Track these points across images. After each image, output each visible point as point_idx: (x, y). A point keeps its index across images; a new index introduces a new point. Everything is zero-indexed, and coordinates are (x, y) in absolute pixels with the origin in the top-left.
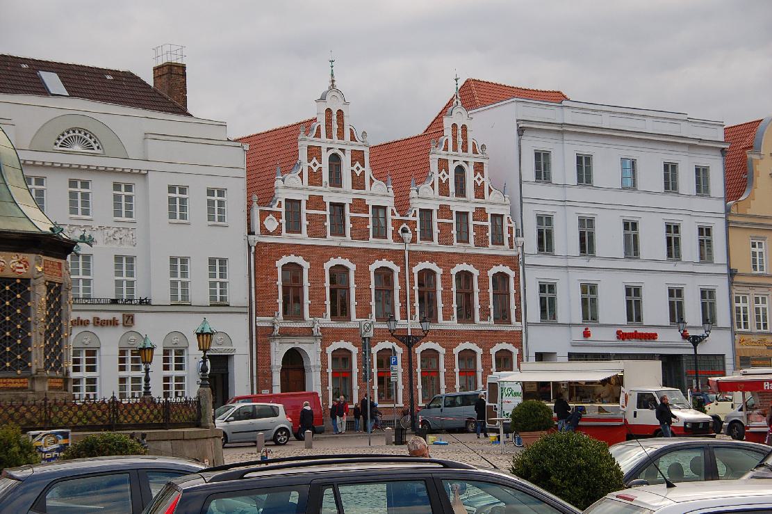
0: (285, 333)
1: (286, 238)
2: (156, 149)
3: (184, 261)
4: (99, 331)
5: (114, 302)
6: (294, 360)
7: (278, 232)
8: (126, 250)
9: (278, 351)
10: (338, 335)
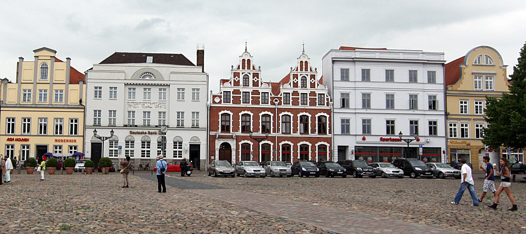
0: (221, 137)
1: (223, 105)
2: (173, 77)
3: (183, 113)
4: (150, 136)
5: (157, 126)
6: (226, 147)
7: (220, 102)
8: (162, 110)
9: (218, 144)
10: (244, 138)
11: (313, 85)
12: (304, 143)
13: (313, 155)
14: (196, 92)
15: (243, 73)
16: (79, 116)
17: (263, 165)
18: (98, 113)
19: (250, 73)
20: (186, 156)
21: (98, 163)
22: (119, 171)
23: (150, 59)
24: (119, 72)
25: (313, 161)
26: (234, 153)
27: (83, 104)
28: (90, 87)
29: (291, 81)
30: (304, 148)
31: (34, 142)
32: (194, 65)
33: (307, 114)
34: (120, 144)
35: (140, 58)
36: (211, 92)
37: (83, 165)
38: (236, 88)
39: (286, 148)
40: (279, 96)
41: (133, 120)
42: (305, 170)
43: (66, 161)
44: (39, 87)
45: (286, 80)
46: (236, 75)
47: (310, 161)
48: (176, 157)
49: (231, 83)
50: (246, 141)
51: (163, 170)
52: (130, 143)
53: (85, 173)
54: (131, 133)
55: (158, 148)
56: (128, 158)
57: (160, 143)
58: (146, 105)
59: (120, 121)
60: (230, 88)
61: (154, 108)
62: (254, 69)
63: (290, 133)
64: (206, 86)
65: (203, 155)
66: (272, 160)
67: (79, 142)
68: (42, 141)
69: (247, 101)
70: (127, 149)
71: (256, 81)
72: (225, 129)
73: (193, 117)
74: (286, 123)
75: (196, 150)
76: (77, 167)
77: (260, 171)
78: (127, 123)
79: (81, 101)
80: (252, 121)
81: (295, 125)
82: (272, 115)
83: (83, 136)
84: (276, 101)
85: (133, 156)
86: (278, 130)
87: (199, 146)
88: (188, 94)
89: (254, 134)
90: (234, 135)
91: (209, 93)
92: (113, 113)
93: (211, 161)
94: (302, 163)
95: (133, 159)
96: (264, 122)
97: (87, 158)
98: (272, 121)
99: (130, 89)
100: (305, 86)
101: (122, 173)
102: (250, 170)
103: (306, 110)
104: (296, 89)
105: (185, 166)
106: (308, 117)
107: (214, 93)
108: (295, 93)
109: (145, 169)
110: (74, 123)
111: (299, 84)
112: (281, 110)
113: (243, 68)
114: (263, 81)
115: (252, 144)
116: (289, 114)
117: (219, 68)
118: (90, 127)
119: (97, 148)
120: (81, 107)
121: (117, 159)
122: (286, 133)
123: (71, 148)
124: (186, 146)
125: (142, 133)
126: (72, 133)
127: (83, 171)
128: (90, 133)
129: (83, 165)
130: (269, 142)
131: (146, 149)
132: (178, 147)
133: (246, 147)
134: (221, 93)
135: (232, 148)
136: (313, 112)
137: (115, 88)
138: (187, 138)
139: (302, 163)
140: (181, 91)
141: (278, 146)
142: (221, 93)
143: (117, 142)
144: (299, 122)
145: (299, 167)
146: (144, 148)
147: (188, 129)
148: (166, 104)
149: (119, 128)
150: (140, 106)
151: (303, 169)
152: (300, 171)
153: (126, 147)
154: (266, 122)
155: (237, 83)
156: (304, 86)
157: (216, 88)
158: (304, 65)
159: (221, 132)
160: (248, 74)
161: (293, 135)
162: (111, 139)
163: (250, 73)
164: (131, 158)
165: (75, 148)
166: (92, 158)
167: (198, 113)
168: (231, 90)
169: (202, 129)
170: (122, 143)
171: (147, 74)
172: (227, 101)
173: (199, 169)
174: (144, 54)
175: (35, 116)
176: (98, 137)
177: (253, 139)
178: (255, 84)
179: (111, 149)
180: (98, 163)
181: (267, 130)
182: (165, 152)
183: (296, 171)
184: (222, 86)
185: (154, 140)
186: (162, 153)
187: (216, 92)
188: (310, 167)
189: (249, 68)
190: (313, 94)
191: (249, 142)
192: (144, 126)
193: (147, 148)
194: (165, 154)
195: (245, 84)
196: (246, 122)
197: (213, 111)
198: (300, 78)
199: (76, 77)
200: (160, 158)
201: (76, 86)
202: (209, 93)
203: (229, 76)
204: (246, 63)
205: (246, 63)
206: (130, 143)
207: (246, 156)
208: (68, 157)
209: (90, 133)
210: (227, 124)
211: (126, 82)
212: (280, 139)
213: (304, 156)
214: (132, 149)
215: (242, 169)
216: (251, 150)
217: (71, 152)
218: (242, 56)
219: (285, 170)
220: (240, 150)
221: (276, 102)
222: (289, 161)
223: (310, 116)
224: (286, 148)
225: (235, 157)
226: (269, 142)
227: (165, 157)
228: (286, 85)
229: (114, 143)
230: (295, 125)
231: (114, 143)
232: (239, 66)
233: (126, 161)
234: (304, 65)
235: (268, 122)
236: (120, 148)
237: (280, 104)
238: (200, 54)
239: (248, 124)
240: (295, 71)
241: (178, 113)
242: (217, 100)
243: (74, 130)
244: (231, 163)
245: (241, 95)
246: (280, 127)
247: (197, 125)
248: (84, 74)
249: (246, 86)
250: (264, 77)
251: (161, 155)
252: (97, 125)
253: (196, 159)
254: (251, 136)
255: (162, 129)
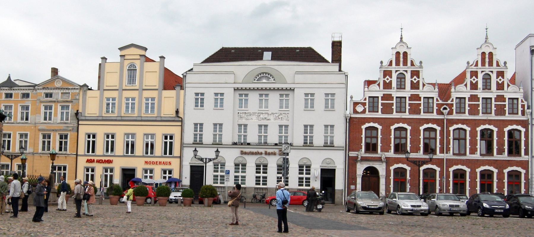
0: (364, 159)
1: (368, 115)
2: (299, 78)
3: (312, 126)
4: (267, 157)
5: (276, 145)
6: (372, 173)
7: (364, 112)
8: (284, 122)
9: (360, 169)
10: (398, 161)
11: (500, 87)
12: (487, 167)
13: (501, 185)
14: (330, 98)
15: (396, 71)
16: (175, 130)
17: (425, 197)
18: (199, 127)
19: (406, 71)
20: (316, 184)
21: (199, 192)
22: (226, 203)
23: (267, 55)
24: (227, 73)
25: (500, 194)
26: (382, 181)
27: (181, 115)
28: (190, 93)
29: (468, 80)
30: (487, 176)
31: (119, 164)
32: (326, 61)
33: (491, 127)
34: (228, 169)
35: (253, 54)
36: (352, 97)
37: (179, 194)
38: (387, 92)
39: (459, 175)
40: (449, 102)
41: (245, 136)
42: (488, 206)
43: (159, 189)
44: (126, 94)
45: (460, 79)
46: (387, 73)
47: (496, 194)
48: (302, 185)
49: (379, 85)
50: (400, 165)
51: (285, 202)
52: (240, 167)
53: (183, 205)
54: (242, 153)
55: (278, 173)
56: (238, 187)
57: (281, 166)
58: (262, 116)
59: (228, 137)
60: (378, 92)
61: (272, 120)
62: (412, 64)
63: (465, 154)
64: (344, 90)
65: (340, 183)
66: (437, 191)
67: (175, 165)
68: (129, 163)
69: (403, 110)
70: (237, 174)
71: (415, 82)
72: (371, 148)
73: (326, 132)
74: (460, 139)
75: (329, 176)
76: (172, 196)
77: (420, 206)
78: (236, 141)
79: (177, 112)
80: (409, 137)
81: (473, 143)
82: (439, 129)
83: (180, 157)
84: (445, 109)
85: (244, 184)
86: (448, 150)
87: (334, 170)
88: (319, 101)
89: (413, 155)
90: (383, 157)
91: (349, 99)
92: (218, 126)
93: (350, 192)
94: (483, 197)
95: (245, 188)
96: (427, 138)
97: (185, 186)
98: (438, 137)
99: (241, 95)
100: (488, 87)
101: (230, 206)
102: (406, 204)
103: (490, 122)
104: (474, 92)
105: (314, 198)
106: (492, 131)
107: (356, 99)
108: (474, 98)
109: (260, 201)
110: (168, 140)
111: (480, 85)
112: (451, 122)
113: (398, 64)
114: (427, 81)
115: (408, 169)
116: (464, 127)
117: (362, 65)
118: (189, 146)
119: (197, 172)
120: (177, 119)
121: (224, 187)
122: (459, 154)
123: (165, 172)
124: (316, 172)
125: (257, 153)
126: (165, 153)
127: (179, 202)
128: (188, 153)
129: (179, 194)
130: (434, 167)
131: (261, 175)
132: (305, 172)
133: (400, 172)
134: (365, 99)
135: (381, 174)
136: (501, 124)
137: (222, 94)
138: (317, 161)
139: (483, 197)
140: (309, 97)
141: (448, 171)
142: (365, 99)
143: (223, 165)
144: (478, 138)
145: (479, 202)
146: (260, 173)
147: (319, 148)
148: (289, 115)
149: (227, 147)
150: (254, 117)
151: (485, 205)
152: (479, 207)
153: (235, 172)
154: (430, 138)
155: (387, 86)
156: (487, 87)
157: (357, 92)
158: (488, 58)
159: (365, 152)
160: (405, 73)
161: (469, 156)
162: (215, 161)
163: (406, 71)
164: (242, 186)
165: (170, 172)
166: (191, 185)
167: (332, 126)
168: (380, 95)
169: (339, 149)
170: (230, 166)
171: (265, 75)
172: (373, 109)
173: (333, 202)
174: (260, 48)
175: (120, 132)
176: (199, 159)
177: (411, 162)
178: (415, 86)
179: (216, 174)
180: (199, 192)
181: (432, 150)
182: (287, 178)
183: (474, 208)
184: (366, 89)
185: (273, 162)
186: (283, 180)
187: (358, 98)
188: (495, 203)
189: (405, 64)
190: (500, 98)
191: (405, 166)
192: (259, 144)
193: (306, 174)
194: (287, 181)
195: (399, 87)
196: (400, 138)
197: (353, 124)
198: (480, 76)
199: (172, 81)
200: (280, 187)
201: (171, 93)
202: (349, 99)
203: (377, 76)
204: (402, 58)
205: (402, 58)
206: (240, 166)
207: (400, 186)
208: (161, 184)
209: (188, 153)
210: (374, 141)
211: (236, 86)
212: (451, 163)
213: (487, 187)
214: (243, 174)
215: (395, 204)
216: (408, 177)
217: (165, 178)
218: (395, 48)
219: (458, 206)
220: (392, 177)
221: (444, 111)
222: (463, 192)
223: (495, 130)
224: (459, 175)
225: (384, 186)
226: (434, 167)
227: (287, 185)
228: (461, 87)
229: (219, 167)
230: (473, 143)
231: (219, 167)
232: (391, 62)
233: (236, 190)
234: (488, 58)
235: (433, 138)
236: (228, 172)
237: (450, 113)
238: (337, 47)
239: (403, 141)
240: (473, 67)
241: (306, 126)
242: (360, 109)
243: (168, 149)
244: (378, 194)
245: (394, 102)
246: (451, 146)
247: (332, 143)
248: (182, 76)
249: (401, 88)
250: (428, 75)
251: (282, 183)
252: (198, 143)
253: (330, 189)
254: (407, 159)
255: (283, 148)
